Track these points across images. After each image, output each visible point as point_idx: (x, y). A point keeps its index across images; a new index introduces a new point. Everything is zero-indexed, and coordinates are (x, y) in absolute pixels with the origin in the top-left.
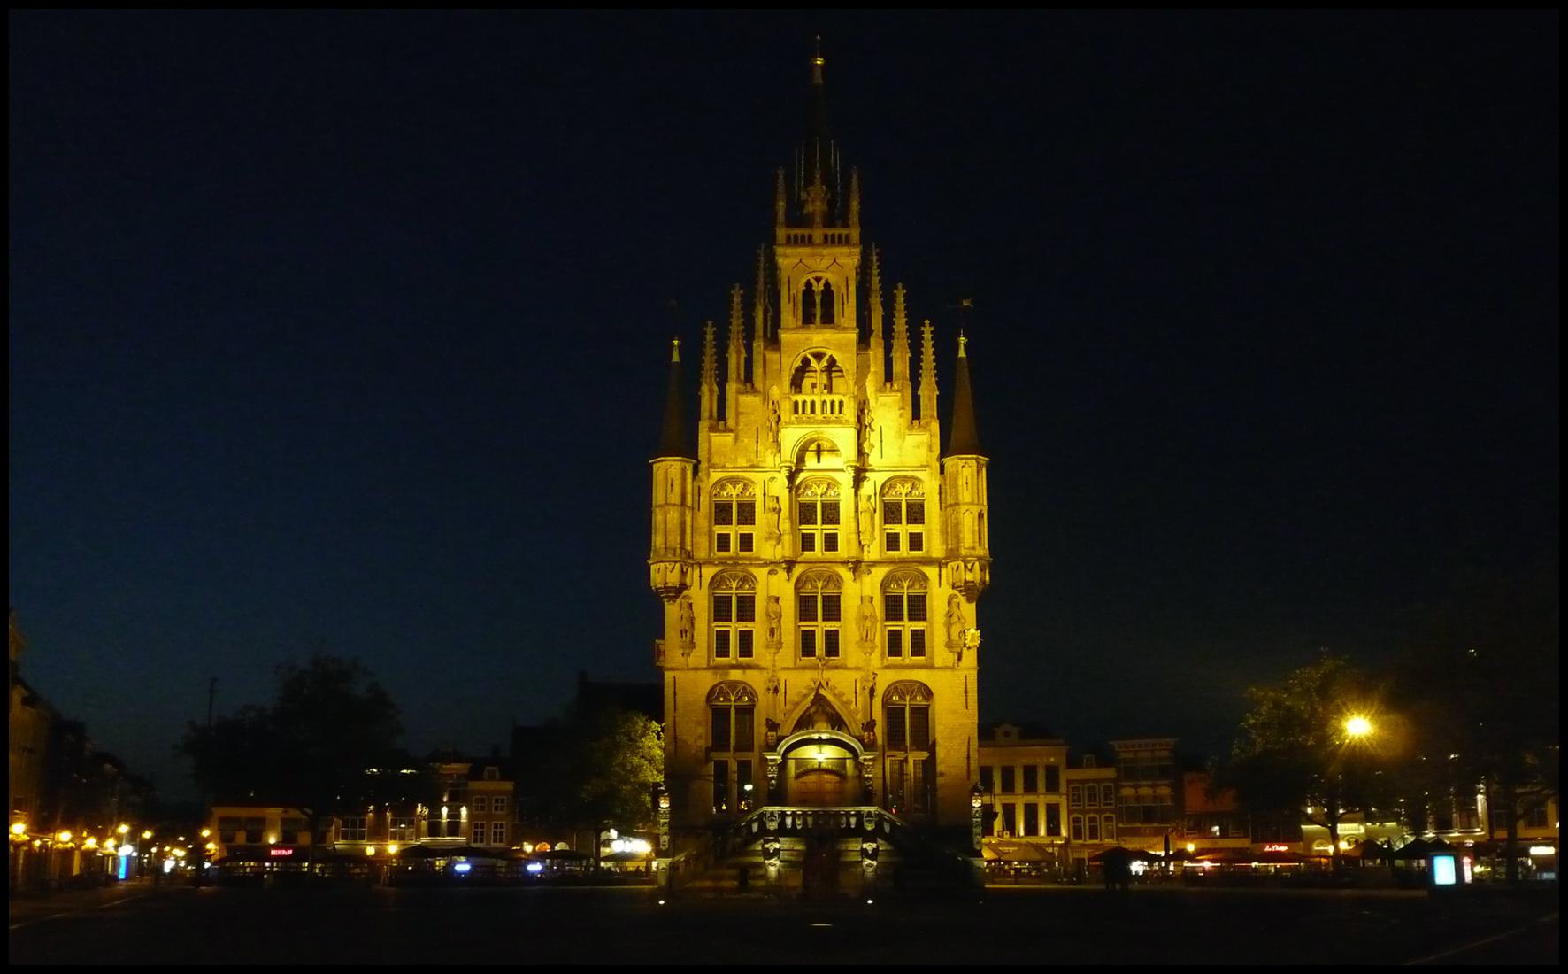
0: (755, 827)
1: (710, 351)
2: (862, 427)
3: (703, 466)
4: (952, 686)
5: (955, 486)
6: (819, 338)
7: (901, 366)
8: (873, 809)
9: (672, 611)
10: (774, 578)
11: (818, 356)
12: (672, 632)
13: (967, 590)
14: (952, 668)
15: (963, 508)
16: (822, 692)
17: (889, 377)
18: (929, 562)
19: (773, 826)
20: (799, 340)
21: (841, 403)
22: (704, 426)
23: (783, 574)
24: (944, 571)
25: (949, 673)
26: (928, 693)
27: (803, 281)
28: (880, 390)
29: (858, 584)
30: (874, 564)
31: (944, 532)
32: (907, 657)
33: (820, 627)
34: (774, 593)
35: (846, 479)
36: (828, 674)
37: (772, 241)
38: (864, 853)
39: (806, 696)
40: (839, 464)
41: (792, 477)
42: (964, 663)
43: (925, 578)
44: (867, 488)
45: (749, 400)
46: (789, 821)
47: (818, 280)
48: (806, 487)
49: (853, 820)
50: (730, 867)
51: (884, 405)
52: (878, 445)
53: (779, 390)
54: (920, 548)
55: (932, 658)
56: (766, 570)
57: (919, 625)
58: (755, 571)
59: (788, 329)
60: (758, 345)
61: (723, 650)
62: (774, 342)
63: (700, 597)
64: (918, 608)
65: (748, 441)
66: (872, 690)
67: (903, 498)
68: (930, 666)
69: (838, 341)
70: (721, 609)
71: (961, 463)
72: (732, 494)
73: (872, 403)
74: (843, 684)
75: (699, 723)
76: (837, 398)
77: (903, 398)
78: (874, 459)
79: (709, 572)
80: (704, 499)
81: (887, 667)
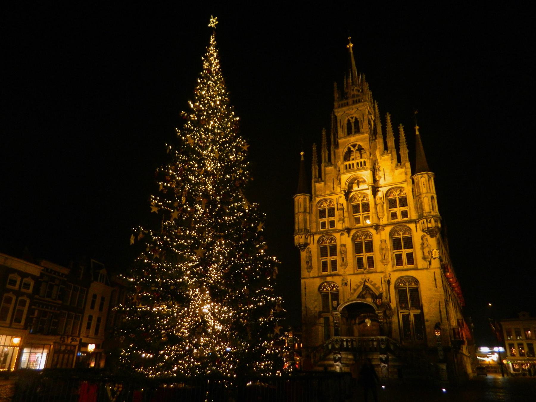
0: (330, 346)
1: (315, 154)
2: (374, 171)
3: (313, 196)
4: (429, 276)
5: (418, 187)
6: (353, 139)
7: (391, 143)
8: (384, 338)
9: (303, 254)
10: (343, 237)
11: (354, 146)
12: (303, 264)
13: (431, 232)
14: (427, 269)
15: (423, 196)
16: (367, 284)
17: (386, 148)
18: (411, 222)
19: (337, 346)
20: (346, 142)
21: (365, 162)
22: (313, 181)
23: (346, 235)
24: (418, 225)
25: (425, 271)
26: (417, 282)
27: (346, 119)
28: (382, 154)
29: (379, 235)
30: (386, 225)
31: (416, 208)
32: (405, 265)
33: (365, 255)
34: (344, 243)
35: (369, 192)
36: (368, 276)
37: (333, 107)
38: (381, 360)
39: (359, 286)
40: (365, 188)
41: (347, 194)
42: (433, 265)
43: (410, 229)
44: (380, 195)
45: (330, 169)
46: (345, 343)
47: (352, 118)
48: (355, 198)
49: (375, 343)
50: (320, 366)
51: (384, 160)
52: (383, 177)
53: (341, 164)
54: (407, 216)
55: (417, 265)
56: (339, 234)
57: (409, 251)
58: (335, 235)
59: (341, 138)
60: (332, 148)
61: (325, 268)
62: (337, 145)
63: (314, 248)
64: (409, 243)
65: (330, 184)
66: (389, 282)
67: (397, 196)
68: (416, 269)
69: (361, 139)
70: (323, 252)
71: (420, 177)
72: (325, 205)
73: (379, 160)
74: (375, 279)
75: (315, 301)
76: (362, 160)
77: (392, 156)
78: (382, 182)
79: (317, 237)
80: (314, 209)
81: (395, 271)
